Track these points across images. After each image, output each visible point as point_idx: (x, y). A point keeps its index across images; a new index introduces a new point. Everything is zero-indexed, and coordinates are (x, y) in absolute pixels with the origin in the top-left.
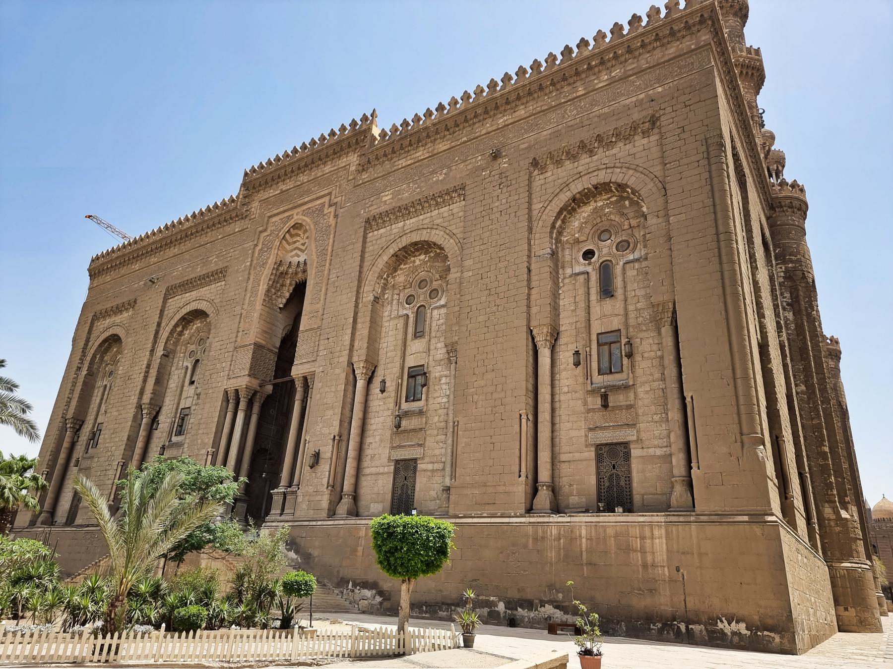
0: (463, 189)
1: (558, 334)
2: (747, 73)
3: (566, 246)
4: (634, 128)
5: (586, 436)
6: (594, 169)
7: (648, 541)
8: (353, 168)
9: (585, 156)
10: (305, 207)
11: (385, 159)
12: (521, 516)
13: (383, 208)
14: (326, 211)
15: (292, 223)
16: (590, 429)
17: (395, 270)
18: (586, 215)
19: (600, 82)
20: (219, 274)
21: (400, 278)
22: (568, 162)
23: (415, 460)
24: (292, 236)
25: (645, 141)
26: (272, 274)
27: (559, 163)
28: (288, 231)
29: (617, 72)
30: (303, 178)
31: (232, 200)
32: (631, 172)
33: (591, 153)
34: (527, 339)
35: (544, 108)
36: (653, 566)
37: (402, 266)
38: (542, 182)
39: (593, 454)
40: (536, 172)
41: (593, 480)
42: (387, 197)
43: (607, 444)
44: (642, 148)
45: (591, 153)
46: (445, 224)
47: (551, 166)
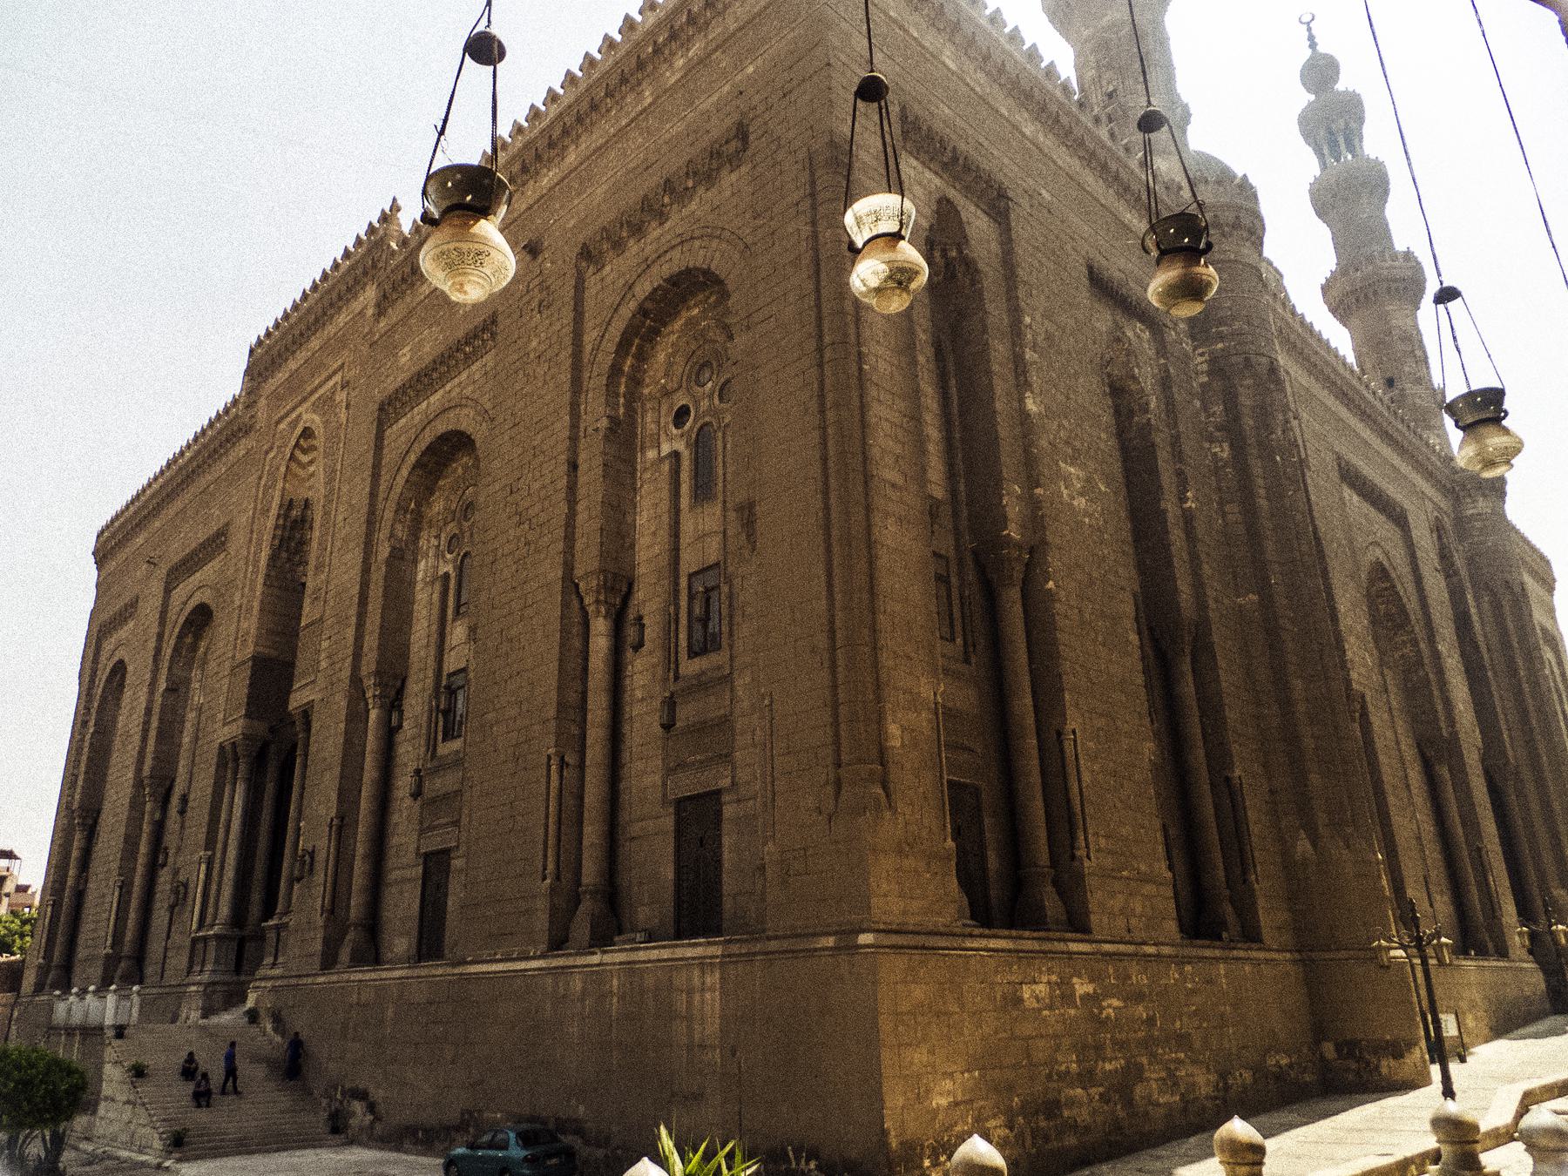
0: (494, 322)
1: (631, 585)
3: (649, 406)
4: (714, 154)
5: (664, 784)
7: (697, 997)
8: (370, 312)
10: (313, 398)
12: (543, 956)
13: (402, 378)
14: (338, 398)
18: (673, 338)
19: (673, 74)
20: (216, 543)
21: (438, 506)
24: (305, 451)
27: (618, 246)
28: (297, 444)
29: (696, 49)
30: (315, 343)
31: (235, 402)
32: (715, 243)
33: (662, 217)
34: (565, 605)
35: (601, 141)
36: (702, 1046)
37: (441, 483)
39: (669, 822)
41: (669, 873)
42: (405, 356)
44: (728, 193)
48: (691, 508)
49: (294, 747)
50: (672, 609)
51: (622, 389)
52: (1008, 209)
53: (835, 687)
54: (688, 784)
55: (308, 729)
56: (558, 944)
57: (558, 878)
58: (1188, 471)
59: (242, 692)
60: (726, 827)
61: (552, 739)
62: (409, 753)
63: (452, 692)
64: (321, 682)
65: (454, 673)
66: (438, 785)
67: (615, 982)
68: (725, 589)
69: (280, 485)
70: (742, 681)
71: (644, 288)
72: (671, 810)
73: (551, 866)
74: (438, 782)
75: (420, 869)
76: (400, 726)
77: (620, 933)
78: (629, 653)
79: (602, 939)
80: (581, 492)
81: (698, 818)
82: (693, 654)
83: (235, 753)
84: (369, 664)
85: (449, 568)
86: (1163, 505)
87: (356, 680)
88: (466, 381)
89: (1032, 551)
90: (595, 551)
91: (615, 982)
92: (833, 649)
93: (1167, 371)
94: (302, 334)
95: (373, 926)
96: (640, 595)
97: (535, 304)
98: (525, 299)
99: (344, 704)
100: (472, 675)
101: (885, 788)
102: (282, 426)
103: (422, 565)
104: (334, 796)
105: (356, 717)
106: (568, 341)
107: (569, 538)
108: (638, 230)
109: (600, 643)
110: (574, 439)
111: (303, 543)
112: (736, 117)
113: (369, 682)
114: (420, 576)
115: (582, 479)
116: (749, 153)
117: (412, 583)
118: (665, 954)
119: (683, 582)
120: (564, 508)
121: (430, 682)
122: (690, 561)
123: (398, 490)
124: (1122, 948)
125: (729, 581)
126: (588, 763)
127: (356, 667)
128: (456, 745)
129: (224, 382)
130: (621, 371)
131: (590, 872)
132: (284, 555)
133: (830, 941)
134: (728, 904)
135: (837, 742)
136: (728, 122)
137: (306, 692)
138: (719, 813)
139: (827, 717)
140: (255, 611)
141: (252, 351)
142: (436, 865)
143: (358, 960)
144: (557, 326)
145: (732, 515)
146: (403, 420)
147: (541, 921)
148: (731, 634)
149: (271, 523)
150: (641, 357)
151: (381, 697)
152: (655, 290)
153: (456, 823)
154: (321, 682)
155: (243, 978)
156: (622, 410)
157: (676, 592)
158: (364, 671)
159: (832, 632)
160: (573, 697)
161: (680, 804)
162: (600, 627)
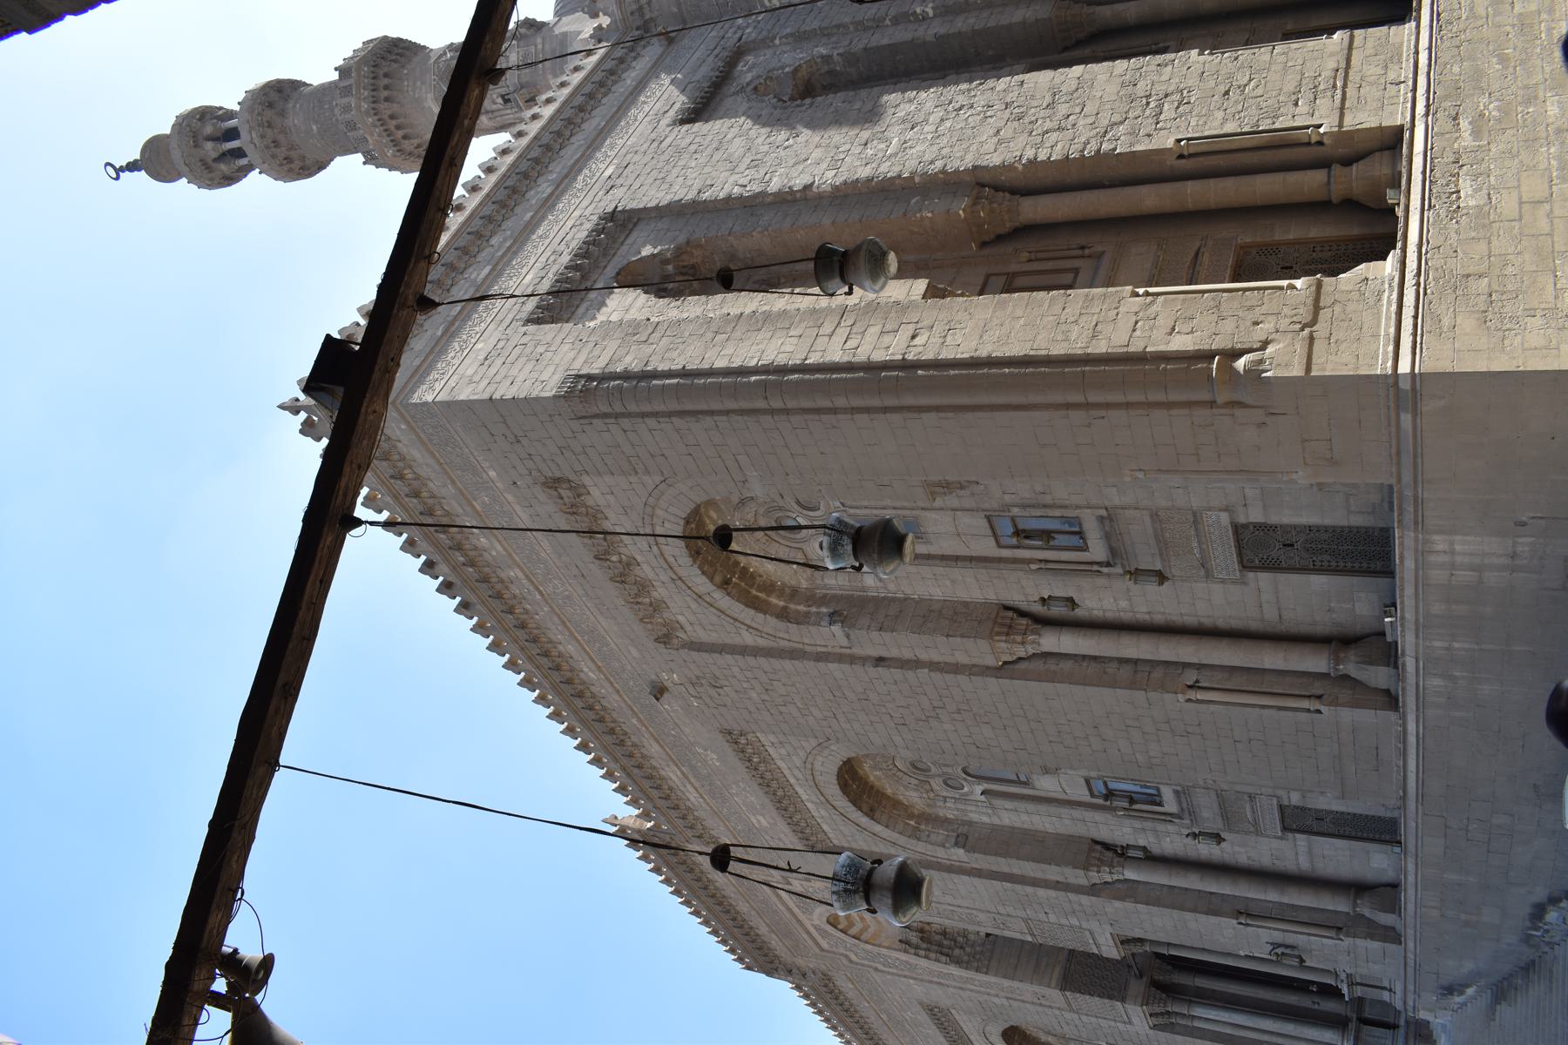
2: (386, 87)
3: (819, 582)
5: (1223, 581)
6: (661, 561)
7: (1459, 559)
9: (637, 570)
11: (690, 817)
12: (1404, 718)
13: (782, 825)
15: (830, 929)
16: (1209, 575)
17: (896, 804)
20: (940, 1018)
21: (913, 797)
22: (655, 594)
23: (1281, 808)
25: (595, 492)
26: (926, 957)
27: (657, 607)
31: (798, 988)
32: (659, 512)
34: (1025, 676)
35: (556, 619)
36: (1514, 556)
37: (889, 792)
38: (698, 629)
39: (1264, 578)
40: (681, 634)
41: (1318, 581)
43: (1240, 555)
45: (630, 563)
46: (802, 754)
47: (665, 615)
48: (928, 542)
49: (1158, 956)
50: (1033, 567)
51: (801, 608)
52: (624, 211)
53: (1128, 405)
54: (1224, 554)
55: (1141, 941)
56: (1391, 700)
57: (1319, 697)
58: (892, 12)
59: (1094, 1002)
60: (1274, 519)
61: (1168, 697)
62: (1172, 841)
63: (1110, 794)
64: (1094, 925)
65: (1090, 790)
66: (1210, 817)
67: (1437, 644)
68: (1015, 511)
69: (884, 951)
70: (1114, 498)
71: (702, 583)
72: (1251, 575)
73: (1305, 704)
74: (1206, 814)
75: (1298, 836)
76: (1144, 849)
77: (1383, 634)
78: (1080, 613)
79: (1390, 655)
80: (907, 654)
81: (1261, 548)
82: (1085, 549)
83: (1162, 1014)
84: (1077, 877)
85: (979, 789)
86: (929, 38)
87: (1093, 890)
88: (786, 762)
89: (983, 186)
90: (969, 643)
91: (1437, 644)
92: (1087, 406)
93: (786, 37)
94: (734, 919)
95: (1358, 888)
96: (1016, 598)
97: (712, 692)
98: (708, 700)
99: (1117, 904)
100: (1093, 774)
101: (1239, 354)
102: (824, 945)
103: (974, 817)
104: (1213, 920)
105: (1129, 891)
106: (751, 660)
107: (956, 669)
108: (643, 587)
109: (1066, 642)
110: (852, 660)
111: (944, 933)
112: (538, 490)
113: (1095, 877)
114: (985, 819)
115: (894, 652)
116: (572, 477)
117: (995, 828)
118: (1409, 590)
119: (1006, 553)
120: (923, 673)
121: (1099, 816)
122: (987, 547)
123: (895, 836)
124: (1421, 89)
125: (1006, 507)
126: (1195, 660)
127: (1079, 890)
128: (1167, 794)
129: (780, 997)
130: (785, 608)
131: (1316, 662)
132: (957, 952)
133: (1406, 419)
134: (1358, 521)
135: (1189, 405)
136: (542, 496)
137: (1101, 940)
138: (1259, 527)
139: (1159, 414)
140: (1016, 984)
141: (748, 968)
142: (1296, 821)
143: (1394, 907)
144: (735, 670)
145: (939, 502)
146: (825, 827)
147: (1366, 717)
148: (1065, 507)
149: (923, 963)
150: (770, 587)
151: (1111, 866)
152: (704, 573)
153: (1251, 797)
154: (1094, 925)
155: (1402, 1023)
156: (824, 610)
157: (1015, 561)
158: (1083, 881)
159: (1068, 406)
160: (1125, 672)
161: (1245, 566)
162: (1051, 641)
